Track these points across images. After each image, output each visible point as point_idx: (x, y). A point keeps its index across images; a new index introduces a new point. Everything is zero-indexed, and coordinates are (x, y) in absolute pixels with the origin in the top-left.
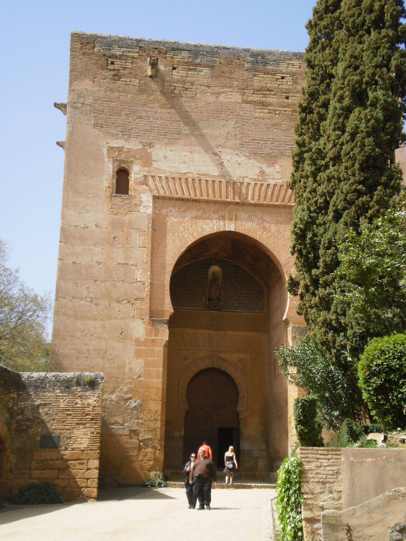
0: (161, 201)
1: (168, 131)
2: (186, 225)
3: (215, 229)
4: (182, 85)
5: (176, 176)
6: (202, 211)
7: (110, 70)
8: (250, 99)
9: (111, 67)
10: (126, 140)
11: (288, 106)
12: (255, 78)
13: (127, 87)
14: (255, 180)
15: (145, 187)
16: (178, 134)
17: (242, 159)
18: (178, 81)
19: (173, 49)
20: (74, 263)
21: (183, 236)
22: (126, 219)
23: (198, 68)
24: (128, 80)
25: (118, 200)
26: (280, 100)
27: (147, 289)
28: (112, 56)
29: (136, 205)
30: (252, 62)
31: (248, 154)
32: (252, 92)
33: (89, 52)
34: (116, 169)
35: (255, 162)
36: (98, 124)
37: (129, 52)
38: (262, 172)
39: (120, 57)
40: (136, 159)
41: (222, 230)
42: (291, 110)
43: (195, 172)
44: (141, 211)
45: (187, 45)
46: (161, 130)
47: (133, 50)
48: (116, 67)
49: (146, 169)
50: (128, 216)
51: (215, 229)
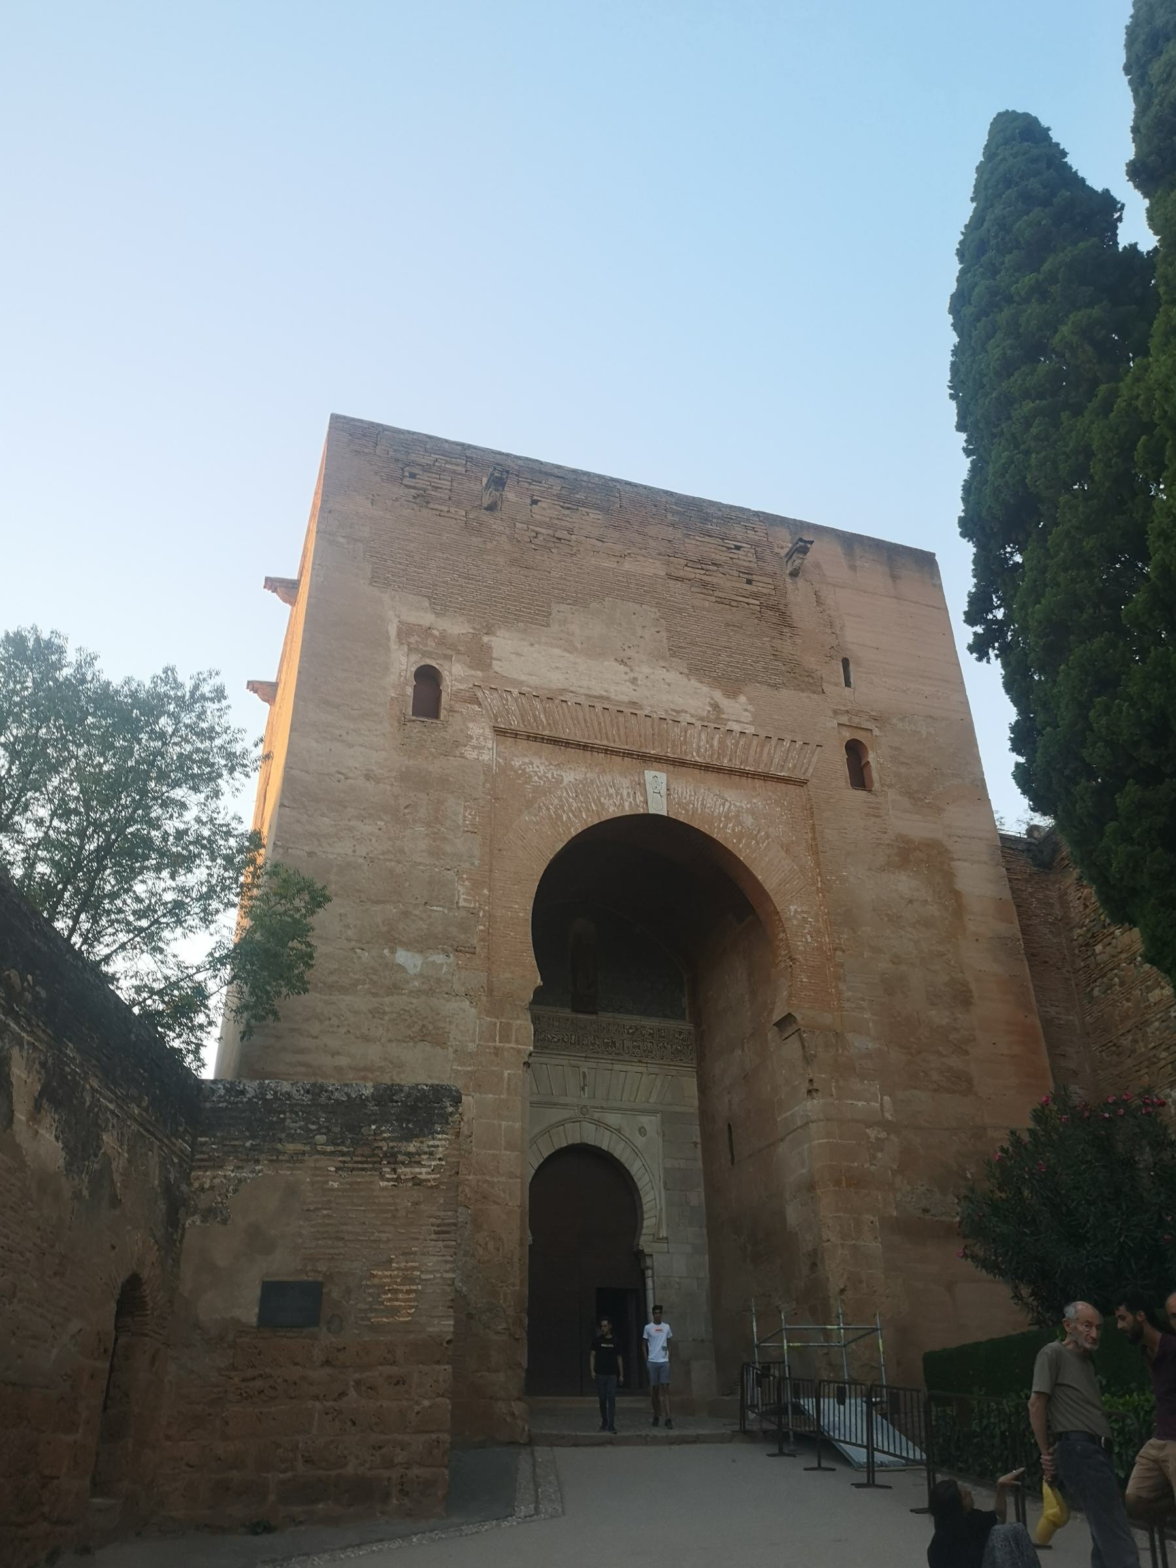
0: (510, 741)
1: (524, 607)
2: (565, 794)
3: (627, 808)
7: (407, 486)
8: (681, 574)
9: (406, 481)
10: (437, 614)
11: (754, 595)
12: (687, 540)
14: (702, 719)
15: (477, 708)
16: (545, 616)
17: (672, 676)
18: (541, 524)
21: (559, 817)
23: (580, 508)
24: (445, 509)
25: (416, 729)
27: (481, 928)
29: (457, 744)
31: (686, 671)
32: (684, 562)
33: (366, 450)
34: (414, 669)
35: (699, 685)
36: (379, 578)
37: (447, 462)
38: (716, 706)
39: (426, 468)
40: (458, 652)
41: (642, 811)
42: (757, 602)
43: (582, 691)
44: (468, 756)
46: (511, 605)
47: (453, 460)
48: (420, 483)
49: (479, 674)
51: (627, 808)
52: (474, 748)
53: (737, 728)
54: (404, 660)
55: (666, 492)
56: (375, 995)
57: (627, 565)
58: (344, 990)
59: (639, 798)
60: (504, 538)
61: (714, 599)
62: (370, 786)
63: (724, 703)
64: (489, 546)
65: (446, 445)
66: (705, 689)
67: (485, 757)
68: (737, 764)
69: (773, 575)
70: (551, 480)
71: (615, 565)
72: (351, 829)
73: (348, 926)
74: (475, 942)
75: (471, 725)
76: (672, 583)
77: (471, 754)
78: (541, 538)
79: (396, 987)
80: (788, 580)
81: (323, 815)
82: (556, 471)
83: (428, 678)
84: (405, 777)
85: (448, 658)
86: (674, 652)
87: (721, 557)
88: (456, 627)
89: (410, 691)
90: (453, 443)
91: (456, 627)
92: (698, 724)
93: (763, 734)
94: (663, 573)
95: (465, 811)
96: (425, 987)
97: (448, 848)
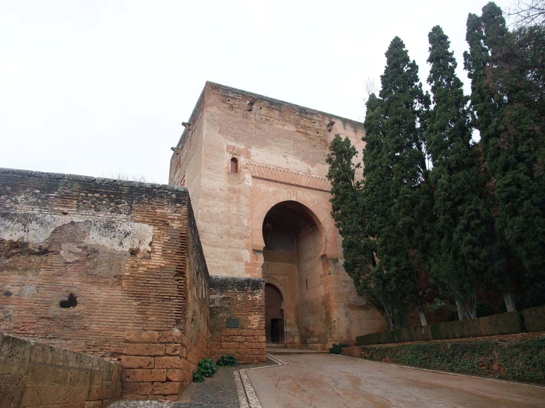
0: (256, 180)
4: (265, 117)
5: (264, 166)
6: (278, 188)
8: (300, 130)
9: (228, 102)
11: (319, 137)
13: (237, 114)
14: (305, 173)
15: (247, 170)
17: (298, 161)
18: (263, 115)
19: (260, 99)
20: (208, 211)
21: (269, 201)
22: (237, 187)
25: (232, 176)
26: (315, 134)
28: (229, 97)
30: (299, 112)
38: (309, 170)
39: (232, 98)
41: (289, 200)
45: (267, 97)
48: (231, 103)
49: (248, 160)
50: (238, 186)
52: (247, 181)
53: (314, 176)
54: (228, 156)
55: (296, 105)
56: (225, 248)
57: (286, 128)
58: (218, 247)
59: (289, 196)
60: (253, 120)
61: (308, 138)
62: (221, 192)
63: (311, 169)
64: (249, 122)
65: (237, 91)
66: (306, 165)
67: (250, 184)
68: (314, 187)
69: (324, 131)
70: (265, 102)
71: (282, 128)
72: (217, 204)
73: (218, 230)
74: (249, 235)
75: (246, 175)
76: (297, 133)
77: (246, 183)
78: (263, 119)
79: (230, 246)
80: (328, 132)
81: (210, 200)
82: (266, 99)
83: (234, 160)
84: (230, 190)
85: (240, 155)
86: (298, 154)
87: (311, 125)
88: (241, 146)
89: (230, 165)
90: (239, 90)
91: (241, 146)
92: (304, 175)
93: (321, 178)
94: (295, 130)
95: (245, 199)
96: (237, 247)
97: (241, 210)
